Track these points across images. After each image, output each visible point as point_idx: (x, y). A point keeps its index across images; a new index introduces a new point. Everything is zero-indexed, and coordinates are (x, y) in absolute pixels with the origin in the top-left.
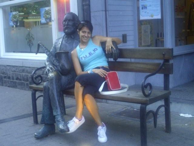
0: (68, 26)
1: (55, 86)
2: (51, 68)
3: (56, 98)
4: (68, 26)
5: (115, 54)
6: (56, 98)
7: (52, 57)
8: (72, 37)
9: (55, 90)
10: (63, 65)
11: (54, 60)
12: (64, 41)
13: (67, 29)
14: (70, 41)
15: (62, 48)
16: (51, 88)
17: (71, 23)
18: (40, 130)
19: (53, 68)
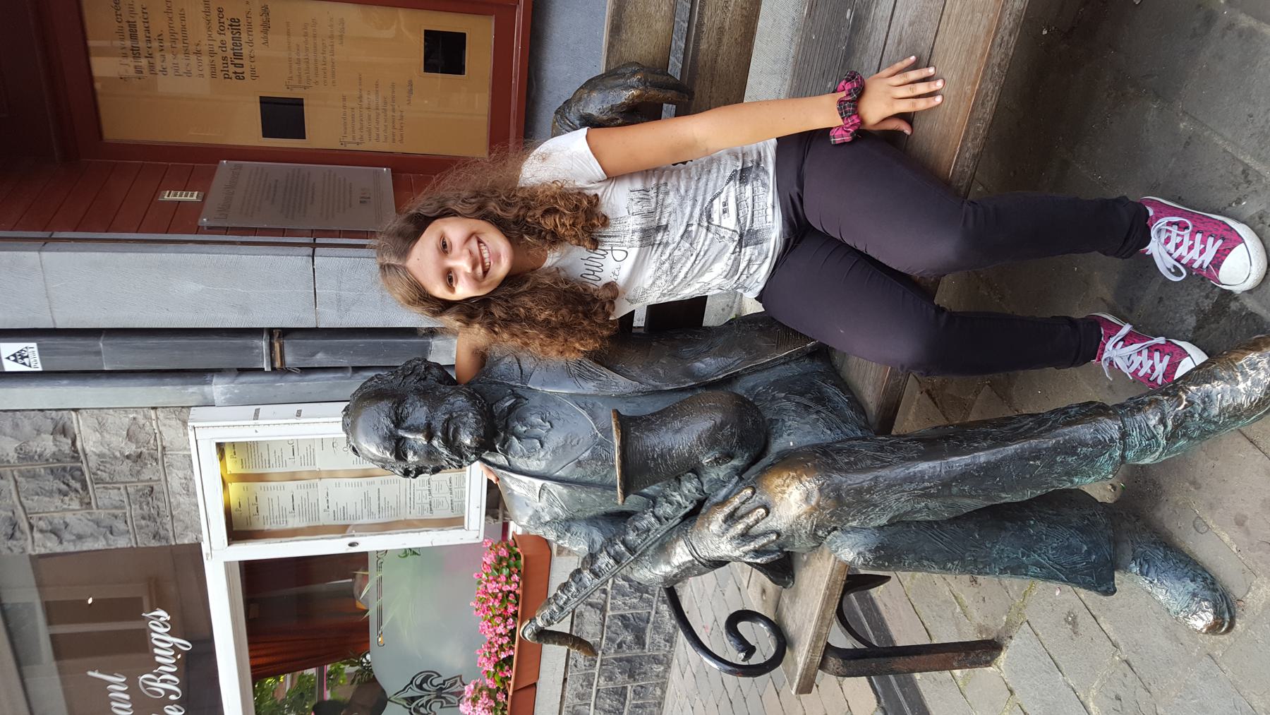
0: (438, 425)
1: (899, 472)
2: (732, 518)
3: (982, 457)
4: (438, 425)
5: (644, 82)
6: (982, 457)
7: (631, 537)
8: (512, 408)
9: (924, 466)
10: (712, 440)
11: (658, 518)
12: (534, 465)
13: (456, 431)
14: (536, 419)
15: (578, 474)
16: (898, 504)
17: (418, 413)
18: (1162, 595)
19: (727, 510)
